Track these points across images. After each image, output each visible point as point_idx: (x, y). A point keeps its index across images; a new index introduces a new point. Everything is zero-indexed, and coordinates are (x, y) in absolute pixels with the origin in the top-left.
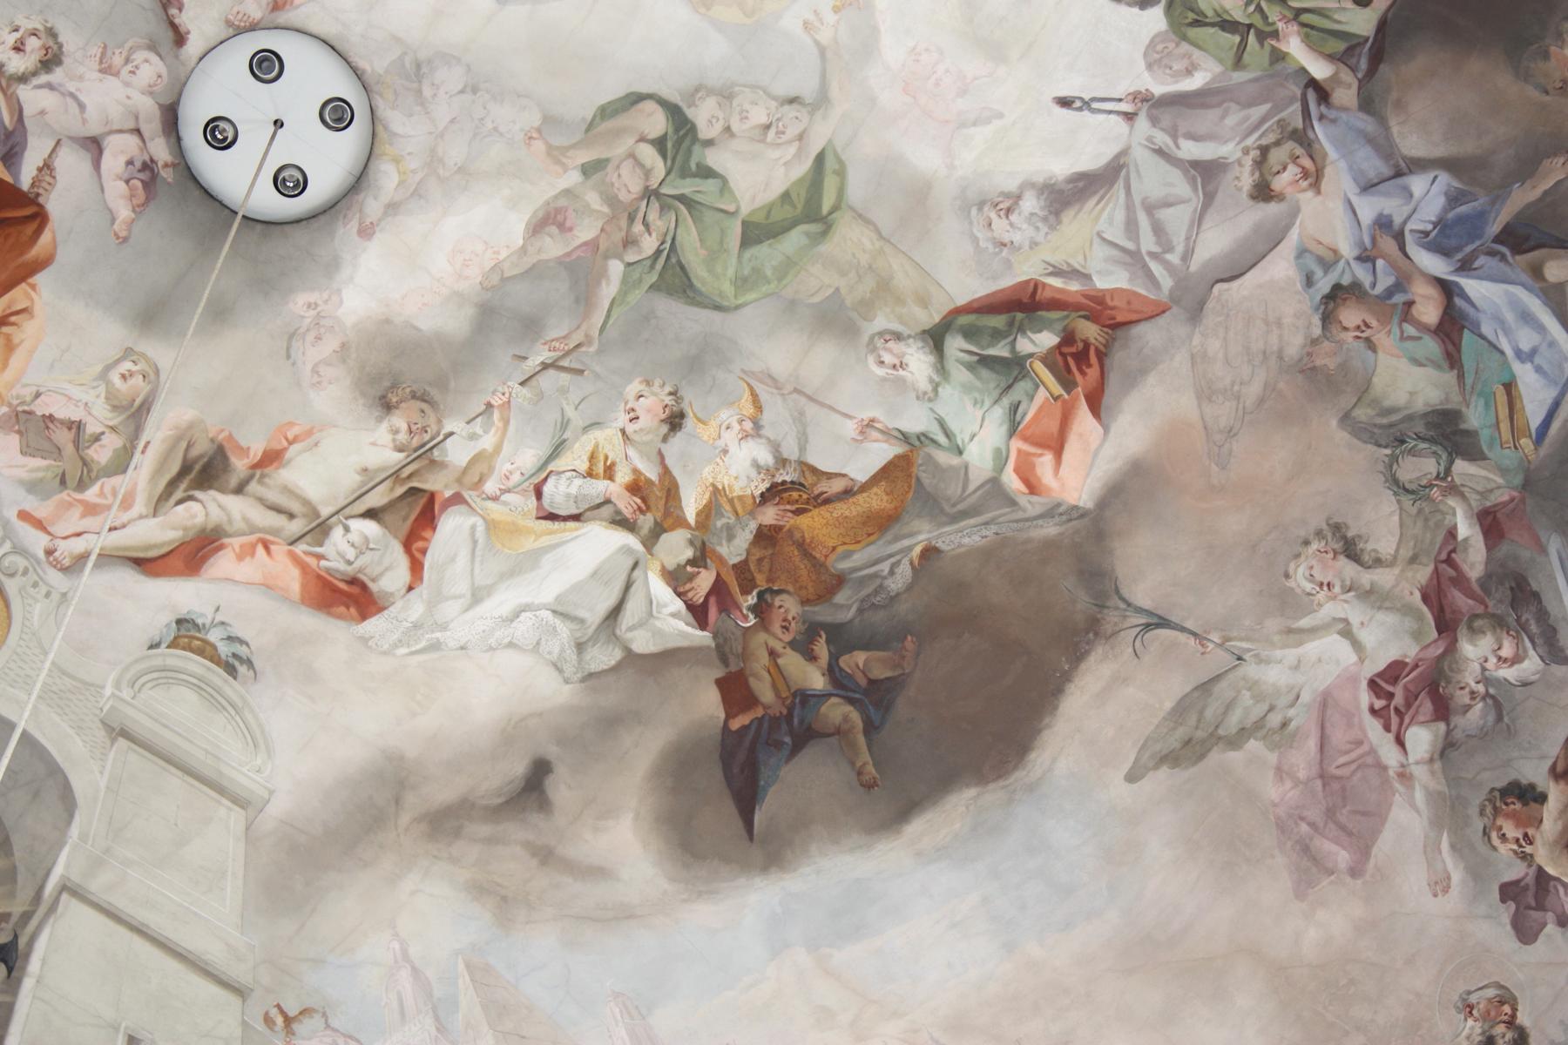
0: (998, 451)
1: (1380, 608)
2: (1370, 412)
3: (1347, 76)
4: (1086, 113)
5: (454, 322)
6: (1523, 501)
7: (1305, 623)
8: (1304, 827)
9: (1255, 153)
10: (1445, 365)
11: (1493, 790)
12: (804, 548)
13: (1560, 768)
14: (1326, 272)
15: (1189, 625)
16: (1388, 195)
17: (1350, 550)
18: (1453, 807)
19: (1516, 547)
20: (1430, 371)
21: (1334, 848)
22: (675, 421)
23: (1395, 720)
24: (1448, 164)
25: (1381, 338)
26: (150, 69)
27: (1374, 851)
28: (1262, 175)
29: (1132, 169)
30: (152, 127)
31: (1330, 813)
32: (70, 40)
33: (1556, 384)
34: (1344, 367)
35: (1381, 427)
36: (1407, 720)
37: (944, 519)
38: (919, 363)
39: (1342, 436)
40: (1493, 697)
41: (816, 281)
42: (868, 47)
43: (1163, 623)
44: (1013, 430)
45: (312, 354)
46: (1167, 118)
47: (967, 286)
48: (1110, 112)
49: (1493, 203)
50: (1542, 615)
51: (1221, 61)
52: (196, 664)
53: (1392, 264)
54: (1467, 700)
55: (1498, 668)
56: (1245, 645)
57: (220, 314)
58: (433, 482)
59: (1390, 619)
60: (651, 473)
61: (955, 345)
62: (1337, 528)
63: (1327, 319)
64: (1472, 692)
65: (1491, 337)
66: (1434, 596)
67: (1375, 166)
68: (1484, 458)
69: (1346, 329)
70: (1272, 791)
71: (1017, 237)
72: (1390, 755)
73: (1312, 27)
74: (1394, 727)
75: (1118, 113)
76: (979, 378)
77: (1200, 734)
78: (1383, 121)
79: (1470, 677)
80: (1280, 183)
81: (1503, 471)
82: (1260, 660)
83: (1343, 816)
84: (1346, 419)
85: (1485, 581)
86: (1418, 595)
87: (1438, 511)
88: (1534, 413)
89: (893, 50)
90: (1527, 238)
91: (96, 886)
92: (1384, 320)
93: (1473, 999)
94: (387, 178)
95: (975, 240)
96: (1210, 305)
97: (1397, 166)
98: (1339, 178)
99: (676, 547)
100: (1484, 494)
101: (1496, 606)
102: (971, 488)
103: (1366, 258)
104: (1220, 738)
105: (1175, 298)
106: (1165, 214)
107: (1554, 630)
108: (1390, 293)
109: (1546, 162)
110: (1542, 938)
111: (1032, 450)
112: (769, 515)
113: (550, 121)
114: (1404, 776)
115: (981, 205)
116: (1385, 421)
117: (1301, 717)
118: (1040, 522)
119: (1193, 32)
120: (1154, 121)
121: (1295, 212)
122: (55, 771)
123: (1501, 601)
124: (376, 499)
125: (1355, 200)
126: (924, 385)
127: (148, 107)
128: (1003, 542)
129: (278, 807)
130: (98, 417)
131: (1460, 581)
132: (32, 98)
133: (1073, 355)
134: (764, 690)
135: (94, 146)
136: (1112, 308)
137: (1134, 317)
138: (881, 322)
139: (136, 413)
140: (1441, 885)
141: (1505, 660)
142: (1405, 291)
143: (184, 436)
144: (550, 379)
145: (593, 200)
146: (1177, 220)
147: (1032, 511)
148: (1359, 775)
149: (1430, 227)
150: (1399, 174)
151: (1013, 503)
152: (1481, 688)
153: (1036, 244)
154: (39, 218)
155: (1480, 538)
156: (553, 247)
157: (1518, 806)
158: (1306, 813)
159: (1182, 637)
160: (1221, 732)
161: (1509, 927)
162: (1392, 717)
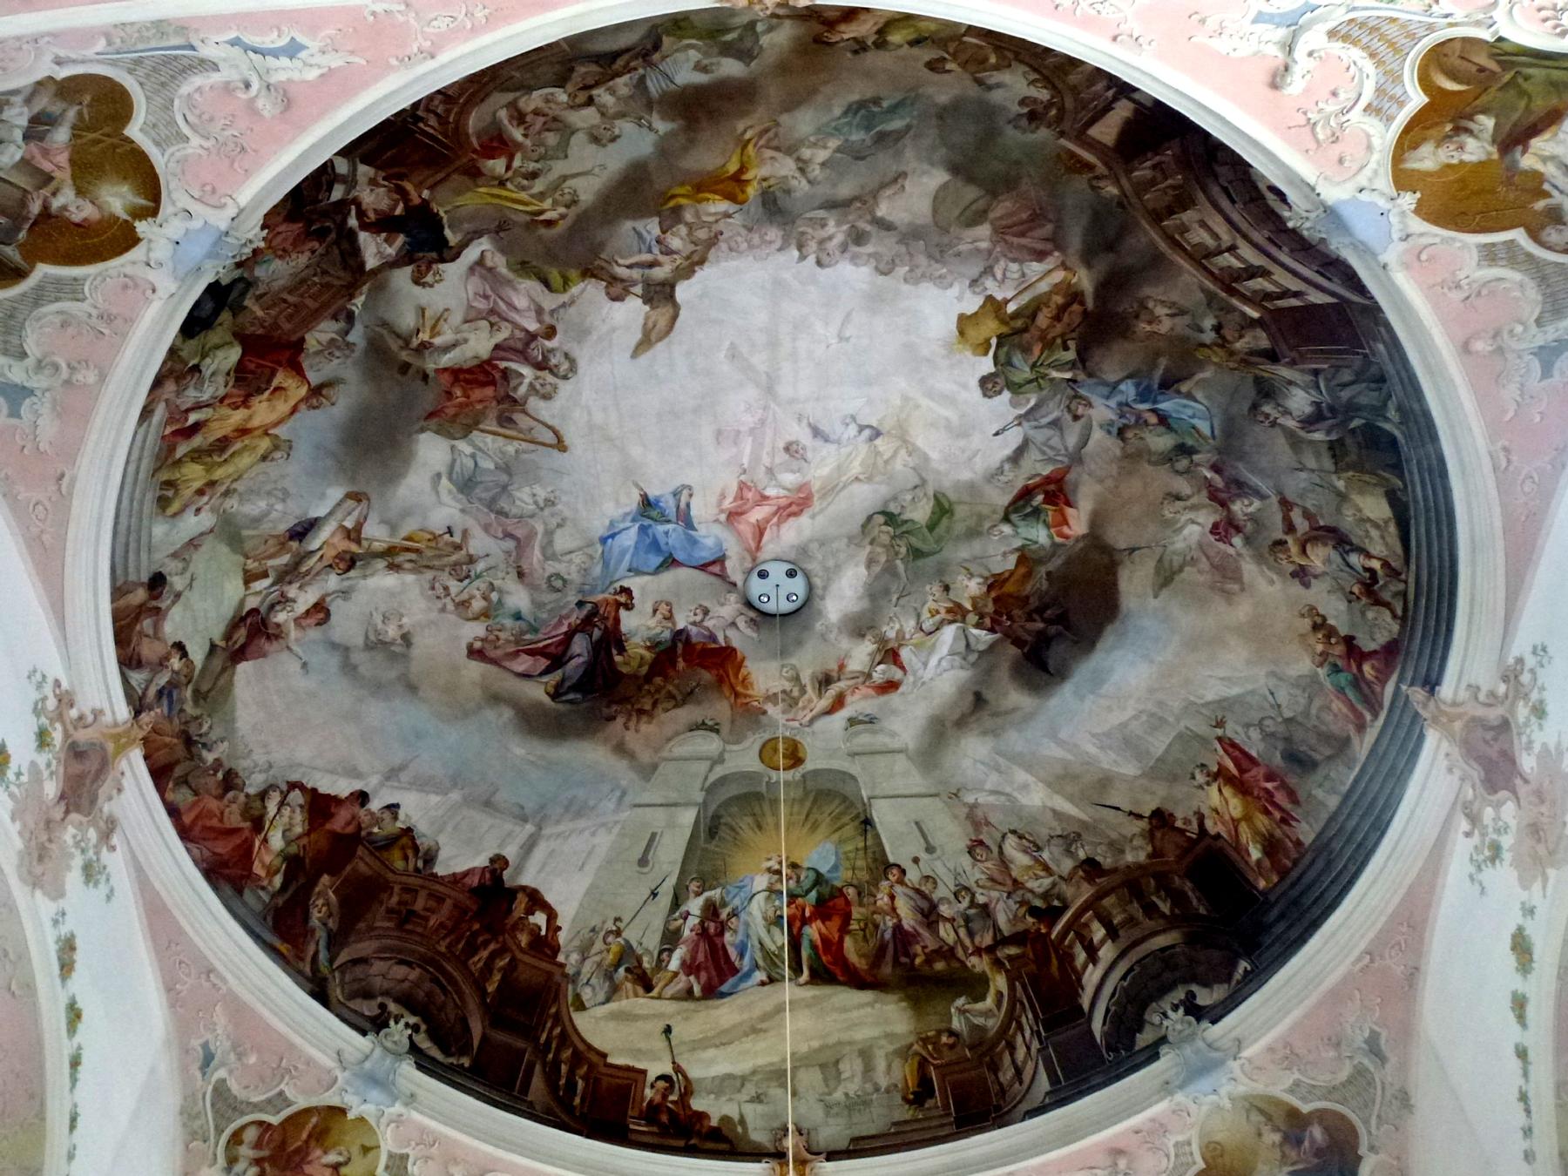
5: (865, 604)
12: (1010, 595)
17: (1178, 498)
22: (947, 588)
24: (1129, 377)
26: (733, 597)
30: (745, 610)
31: (1224, 577)
32: (706, 604)
38: (1007, 529)
41: (959, 528)
42: (926, 458)
43: (1132, 550)
44: (1048, 527)
45: (832, 636)
47: (1004, 500)
50: (1250, 487)
52: (861, 727)
57: (799, 643)
58: (890, 646)
59: (1204, 511)
60: (950, 605)
61: (1014, 517)
62: (1169, 494)
63: (1123, 440)
67: (1105, 391)
70: (1201, 579)
72: (1231, 551)
79: (1240, 516)
80: (1080, 411)
84: (1149, 462)
89: (934, 455)
91: (877, 792)
94: (817, 581)
98: (1097, 401)
99: (972, 618)
103: (1122, 416)
112: (993, 594)
113: (851, 539)
114: (1239, 555)
117: (1196, 554)
121: (1090, 418)
122: (844, 773)
124: (878, 658)
127: (739, 606)
129: (911, 746)
130: (787, 686)
131: (1218, 490)
132: (709, 623)
134: (1029, 638)
135: (733, 624)
138: (987, 525)
139: (796, 679)
143: (813, 677)
144: (902, 601)
145: (879, 550)
146: (1055, 441)
154: (734, 650)
156: (877, 569)
162: (1225, 539)
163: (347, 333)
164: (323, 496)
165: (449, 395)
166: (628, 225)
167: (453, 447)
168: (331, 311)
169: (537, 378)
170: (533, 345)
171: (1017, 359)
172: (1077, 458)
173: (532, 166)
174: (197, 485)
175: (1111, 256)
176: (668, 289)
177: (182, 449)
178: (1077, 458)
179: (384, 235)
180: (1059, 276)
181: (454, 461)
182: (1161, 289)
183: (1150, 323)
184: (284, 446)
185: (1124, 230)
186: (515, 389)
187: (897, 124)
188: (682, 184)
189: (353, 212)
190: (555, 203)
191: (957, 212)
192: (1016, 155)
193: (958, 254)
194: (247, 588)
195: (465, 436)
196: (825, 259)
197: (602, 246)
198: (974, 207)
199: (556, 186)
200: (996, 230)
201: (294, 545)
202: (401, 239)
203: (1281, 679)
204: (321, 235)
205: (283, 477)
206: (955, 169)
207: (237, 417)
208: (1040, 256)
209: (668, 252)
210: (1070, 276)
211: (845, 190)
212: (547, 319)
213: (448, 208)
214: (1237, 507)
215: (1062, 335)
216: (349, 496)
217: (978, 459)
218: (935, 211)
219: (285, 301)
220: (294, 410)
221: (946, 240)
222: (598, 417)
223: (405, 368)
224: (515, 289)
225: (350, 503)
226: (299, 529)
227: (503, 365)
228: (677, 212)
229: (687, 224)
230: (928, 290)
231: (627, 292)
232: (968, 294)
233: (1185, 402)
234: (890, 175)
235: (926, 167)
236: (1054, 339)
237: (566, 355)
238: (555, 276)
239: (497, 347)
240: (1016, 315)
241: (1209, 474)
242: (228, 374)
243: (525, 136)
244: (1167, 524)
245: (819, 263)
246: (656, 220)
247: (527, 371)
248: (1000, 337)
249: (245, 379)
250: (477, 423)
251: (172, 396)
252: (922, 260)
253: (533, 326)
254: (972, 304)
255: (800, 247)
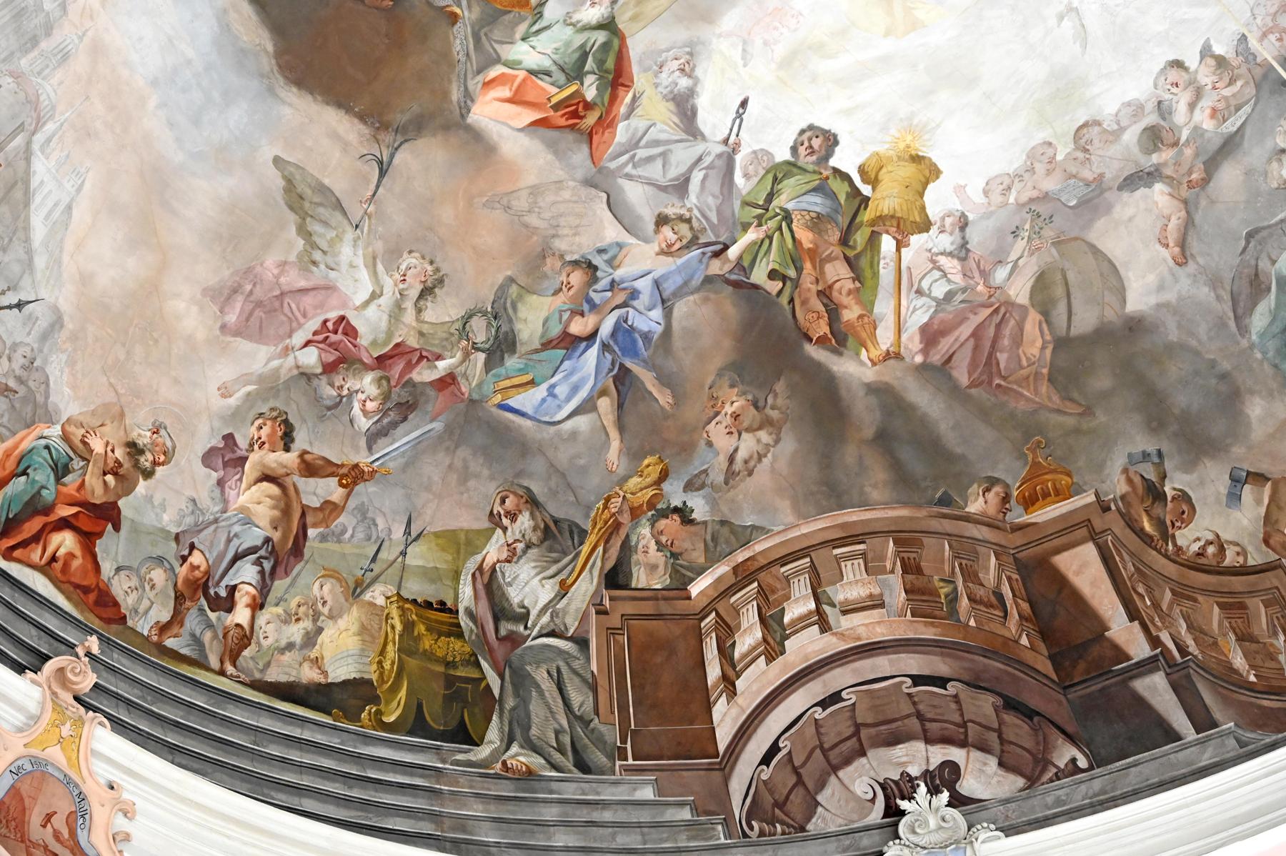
0: (520, 63)
1: (390, 316)
2: (514, 296)
3: (727, 267)
4: (734, 115)
6: (462, 401)
7: (380, 267)
8: (248, 287)
9: (687, 215)
10: (544, 340)
11: (286, 413)
13: (307, 457)
14: (606, 261)
15: (381, 190)
16: (652, 295)
17: (426, 292)
18: (272, 388)
19: (436, 401)
20: (540, 330)
21: (238, 310)
23: (320, 337)
24: (667, 332)
25: (561, 297)
27: (239, 339)
28: (674, 219)
29: (693, 143)
31: (259, 304)
33: (536, 413)
34: (545, 276)
35: (505, 303)
36: (321, 346)
37: (477, 28)
38: (592, 14)
39: (500, 279)
40: (341, 401)
43: (382, 173)
44: (532, 72)
46: (720, 163)
48: (731, 130)
49: (644, 361)
50: (394, 425)
51: (749, 193)
53: (608, 301)
54: (337, 384)
55: (359, 401)
56: (366, 229)
59: (384, 324)
61: (601, 37)
62: (441, 281)
63: (576, 263)
64: (342, 387)
65: (562, 368)
66: (400, 350)
67: (669, 287)
68: (487, 373)
69: (568, 275)
70: (270, 261)
71: (664, 75)
72: (299, 338)
73: (760, 246)
74: (316, 338)
75: (730, 135)
76: (574, 51)
77: (307, 205)
78: (697, 290)
79: (352, 384)
80: (667, 232)
81: (480, 385)
82: (355, 240)
83: (259, 313)
84: (511, 280)
85: (410, 383)
86: (399, 340)
87: (453, 348)
88: (519, 400)
90: (623, 384)
92: (573, 299)
93: (163, 432)
95: (668, 50)
96: (593, 191)
97: (669, 300)
98: (665, 266)
100: (465, 375)
101: (398, 394)
102: (496, 46)
104: (304, 219)
105: (601, 170)
106: (659, 163)
107: (386, 435)
108: (590, 301)
109: (668, 391)
110: (208, 470)
111: (516, 85)
114: (287, 350)
115: (691, 54)
116: (508, 305)
118: (462, 89)
119: (770, 177)
120: (719, 156)
121: (646, 241)
123: (399, 396)
125: (650, 277)
126: (576, 17)
128: (452, 65)
131: (410, 366)
133: (577, 109)
136: (603, 133)
137: (594, 146)
140: (225, 392)
141: (364, 405)
142: (590, 311)
146: (654, 171)
147: (471, 84)
148: (285, 319)
149: (630, 323)
150: (663, 301)
151: (479, 72)
152: (345, 392)
153: (656, 87)
155: (438, 377)
157: (280, 433)
158: (258, 286)
159: (373, 187)
160: (309, 219)
161: (209, 446)
162: (322, 337)
171: (817, 203)
172: (599, 181)
175: (869, 433)
178: (599, 181)
180: (885, 338)
182: (783, 465)
183: (736, 416)
185: (903, 482)
187: (1259, 319)
191: (1071, 276)
192: (1101, 417)
193: (1015, 233)
196: (1174, 75)
198: (1062, 307)
200: (1010, 304)
203: (44, 337)
206: (1135, 326)
208: (930, 336)
210: (875, 353)
211: (1229, 176)
214: (367, 385)
215: (796, 283)
217: (736, 54)
218: (1095, 251)
221: (1048, 233)
230: (1013, 161)
232: (956, 205)
233: (583, 394)
234: (1194, 245)
235: (1170, 296)
236: (799, 270)
240: (874, 240)
241: (443, 366)
244: (393, 255)
245: (1178, 64)
248: (867, 199)
252: (1050, 185)
254: (938, 200)
255: (1221, 62)
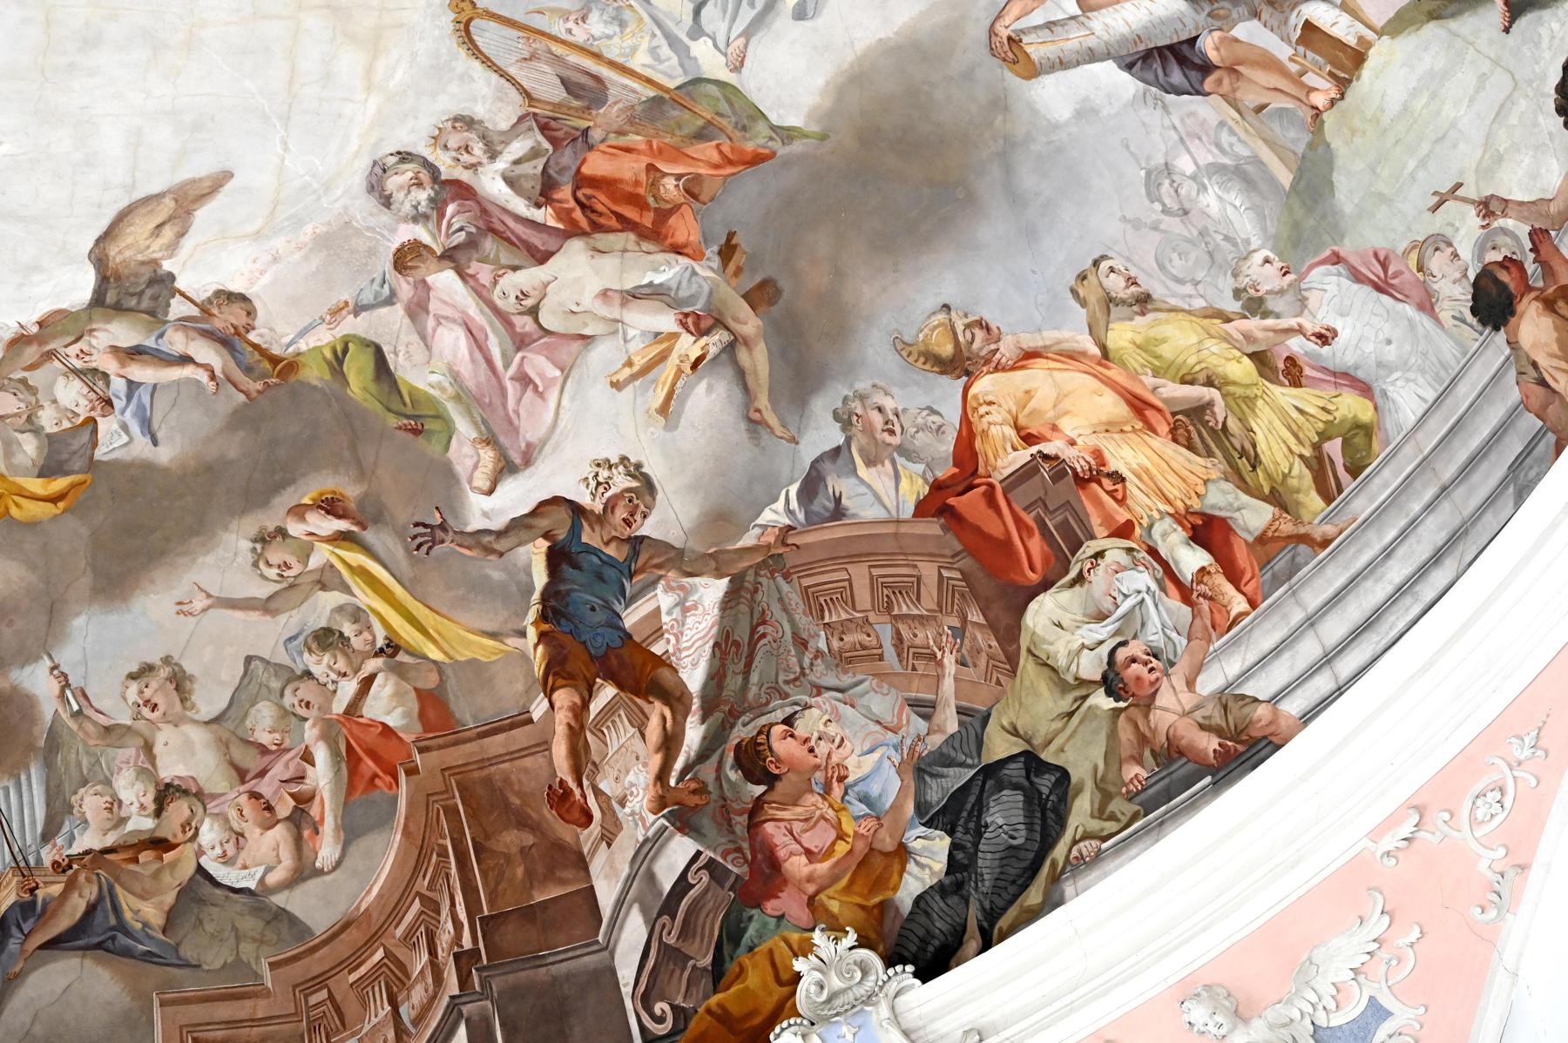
163: (837, 451)
164: (1085, 112)
165: (692, 189)
166: (164, 455)
167: (738, 67)
168: (835, 532)
169: (473, 167)
170: (462, 236)
173: (320, 664)
174: (1284, 395)
176: (110, 298)
177: (1253, 517)
179: (657, 649)
181: (748, 34)
184: (1090, 291)
186: (535, 153)
188: (32, 525)
189: (679, 765)
190: (305, 552)
194: (1366, 44)
195: (698, 81)
197: (238, 420)
199: (289, 592)
201: (1209, 45)
202: (632, 617)
204: (754, 761)
205: (1136, 224)
207: (1125, 456)
209: (91, 376)
212: (405, 289)
213: (513, 642)
216: (1033, 71)
219: (899, 640)
220: (1031, 355)
222: (350, 62)
223: (761, 296)
224: (456, 377)
225: (1036, 49)
226: (1177, 77)
227: (545, 215)
228: (47, 471)
229: (37, 431)
231: (205, 308)
237: (387, 202)
238: (358, 372)
239: (542, 257)
242: (1080, 579)
243: (308, 758)
246: (100, 454)
247: (492, 185)
249: (1064, 527)
250: (656, 102)
251: (1178, 678)
253: (445, 280)
